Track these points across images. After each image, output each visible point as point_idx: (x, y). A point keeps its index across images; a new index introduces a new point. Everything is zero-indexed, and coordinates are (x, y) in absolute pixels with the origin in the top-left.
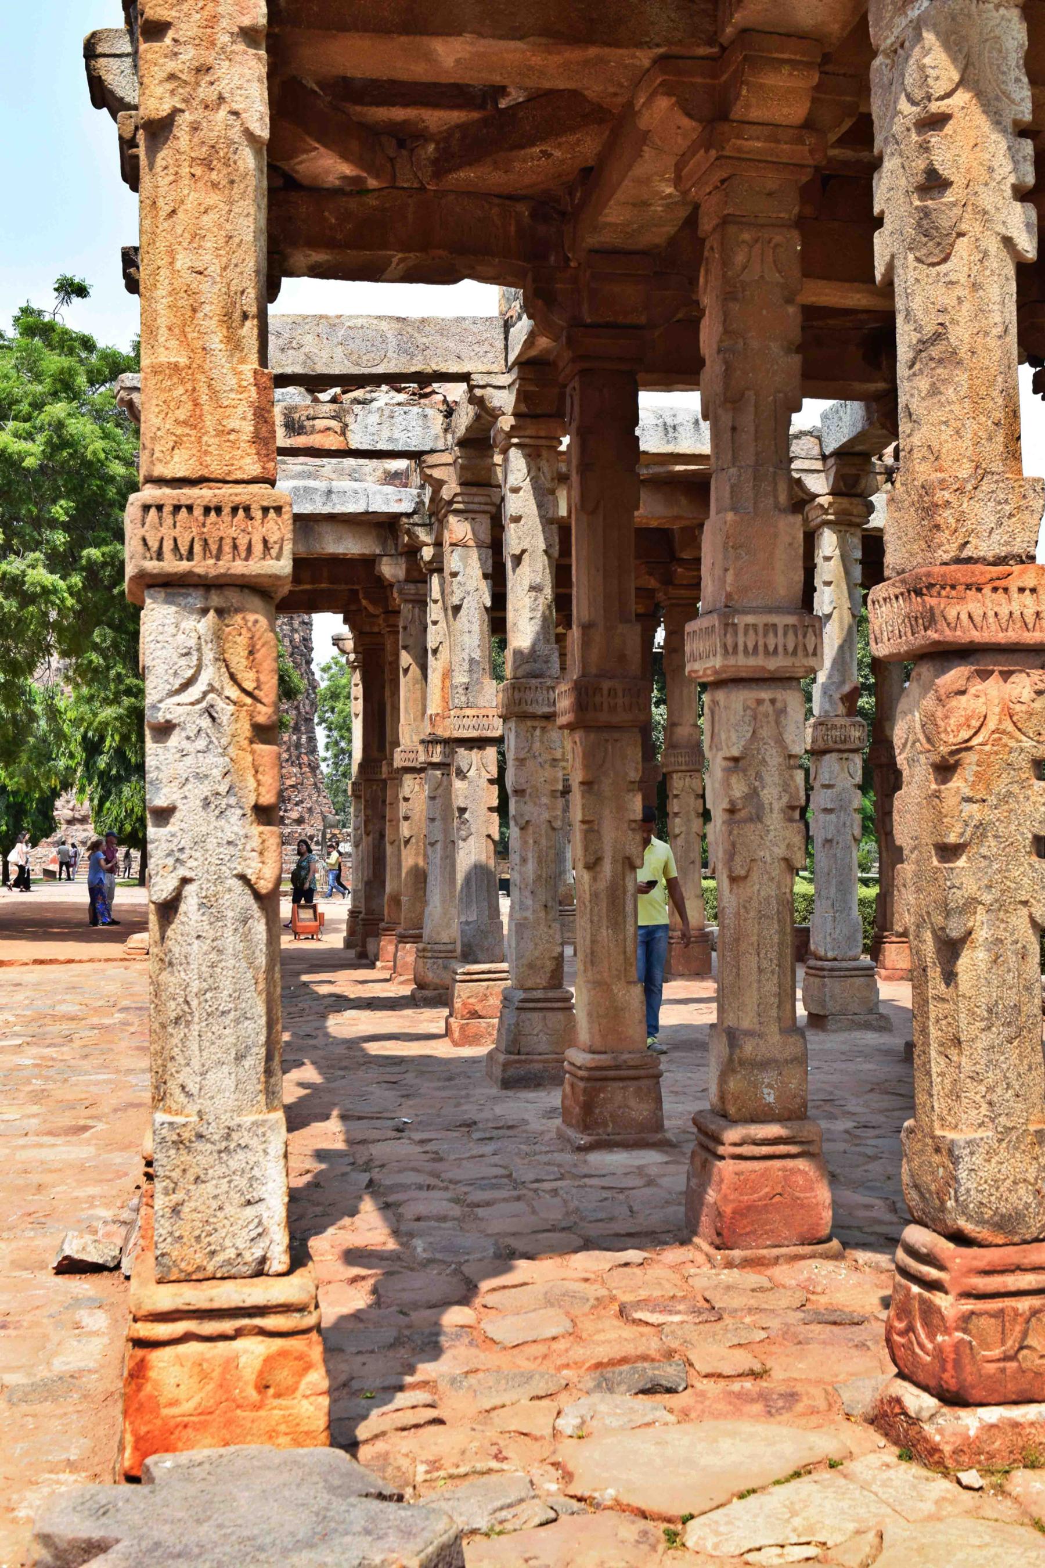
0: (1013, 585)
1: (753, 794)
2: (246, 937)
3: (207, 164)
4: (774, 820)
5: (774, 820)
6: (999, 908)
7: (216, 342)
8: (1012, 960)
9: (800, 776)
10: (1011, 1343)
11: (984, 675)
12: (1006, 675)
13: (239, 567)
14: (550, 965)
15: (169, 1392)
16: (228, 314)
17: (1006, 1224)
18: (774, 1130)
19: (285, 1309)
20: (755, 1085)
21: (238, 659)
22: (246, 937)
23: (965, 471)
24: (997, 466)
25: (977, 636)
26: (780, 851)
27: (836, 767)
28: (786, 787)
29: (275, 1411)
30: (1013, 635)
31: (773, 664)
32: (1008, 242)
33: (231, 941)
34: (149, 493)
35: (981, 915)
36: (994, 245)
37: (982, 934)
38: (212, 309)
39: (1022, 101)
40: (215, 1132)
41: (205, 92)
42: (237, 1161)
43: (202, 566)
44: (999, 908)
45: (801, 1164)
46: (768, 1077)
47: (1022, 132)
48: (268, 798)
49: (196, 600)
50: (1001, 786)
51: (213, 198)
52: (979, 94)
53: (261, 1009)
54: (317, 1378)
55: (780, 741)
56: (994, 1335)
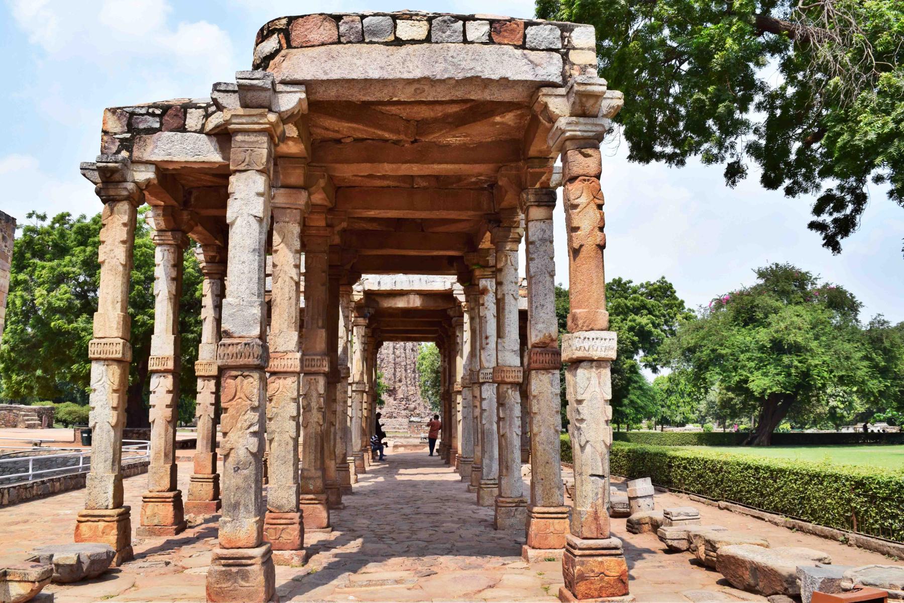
0: (286, 357)
1: (309, 404)
2: (109, 435)
3: (111, 270)
4: (315, 411)
5: (315, 411)
6: (281, 433)
7: (110, 308)
8: (284, 445)
9: (322, 399)
10: (277, 536)
11: (280, 378)
12: (285, 378)
13: (111, 356)
14: (342, 456)
15: (83, 532)
16: (113, 302)
17: (278, 508)
18: (311, 496)
19: (109, 516)
20: (308, 484)
21: (110, 375)
22: (109, 435)
23: (277, 331)
24: (285, 330)
25: (276, 370)
26: (316, 420)
27: (467, 392)
28: (318, 402)
29: (105, 537)
30: (285, 369)
31: (313, 369)
32: (292, 278)
33: (105, 436)
34: (95, 341)
35: (276, 434)
36: (287, 279)
37: (276, 439)
38: (109, 301)
39: (297, 245)
40: (99, 477)
41: (112, 255)
42: (103, 484)
43: (102, 356)
44: (281, 433)
45: (319, 506)
46: (311, 482)
47: (298, 252)
48: (115, 405)
49: (102, 363)
50: (282, 404)
51: (112, 278)
52: (287, 245)
53: (111, 451)
54: (115, 532)
55: (317, 390)
56: (273, 534)
